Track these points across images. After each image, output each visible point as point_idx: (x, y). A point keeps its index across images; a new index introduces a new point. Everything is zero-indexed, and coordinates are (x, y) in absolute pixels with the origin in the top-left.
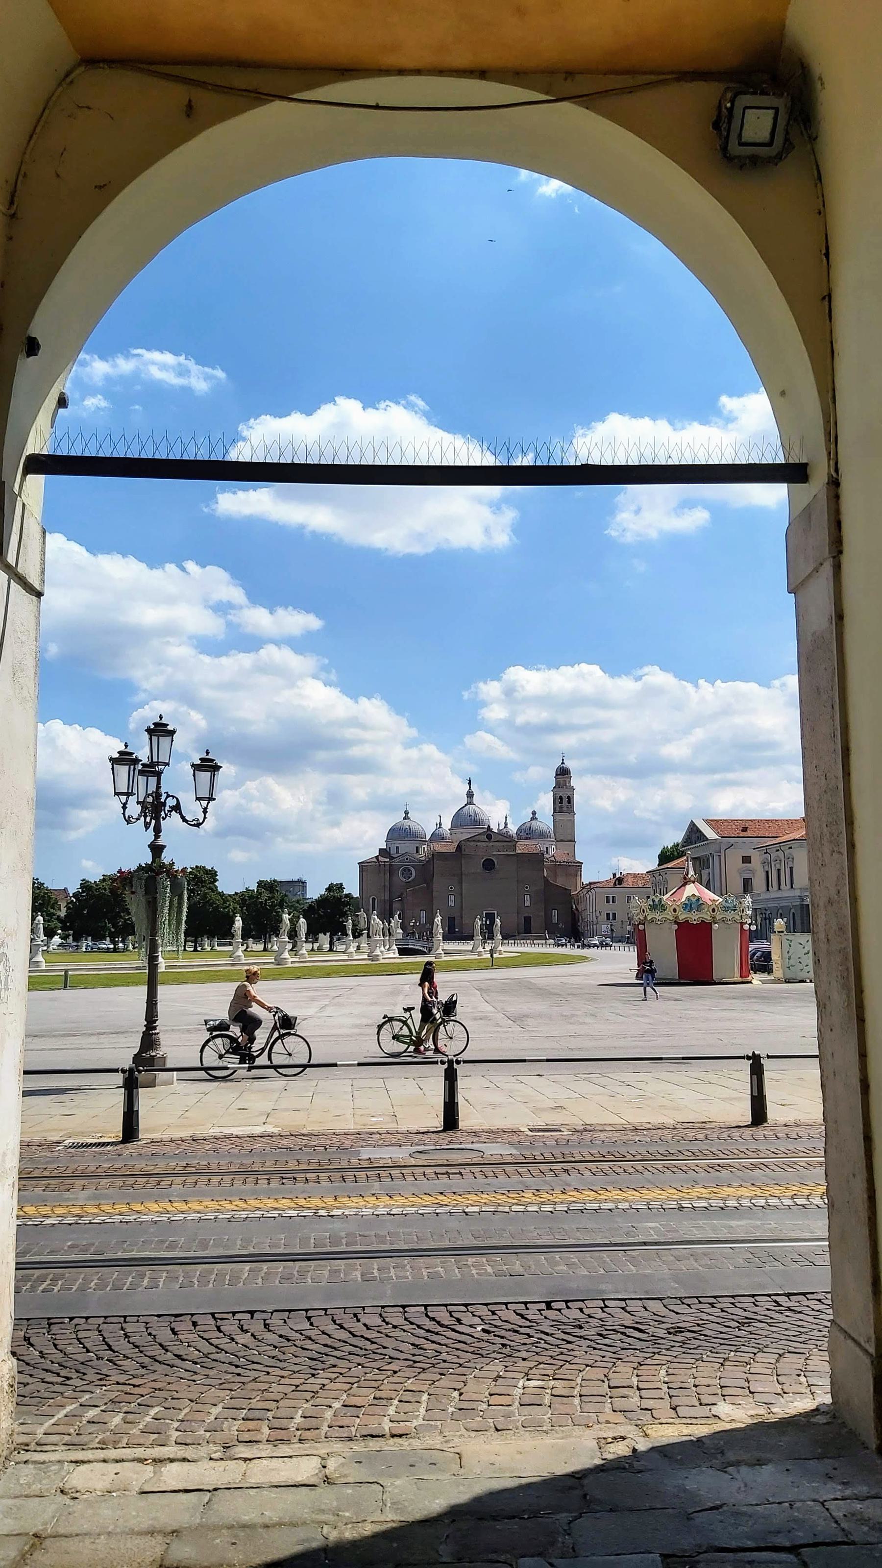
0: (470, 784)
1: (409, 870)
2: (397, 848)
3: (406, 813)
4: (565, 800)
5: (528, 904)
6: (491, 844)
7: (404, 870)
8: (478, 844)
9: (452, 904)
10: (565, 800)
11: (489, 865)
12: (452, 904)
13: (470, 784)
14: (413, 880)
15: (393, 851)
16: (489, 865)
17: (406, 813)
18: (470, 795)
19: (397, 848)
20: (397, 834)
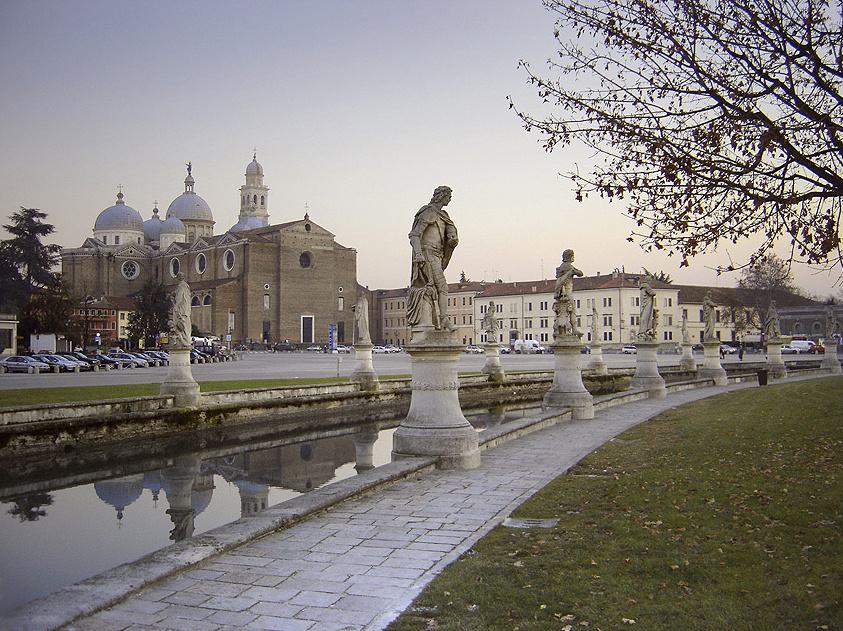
0: (189, 169)
1: (132, 266)
2: (117, 238)
3: (120, 196)
4: (259, 201)
5: (341, 308)
7: (126, 265)
9: (267, 306)
10: (259, 201)
11: (306, 259)
12: (267, 306)
13: (189, 169)
16: (306, 259)
17: (120, 196)
18: (189, 182)
19: (117, 238)
20: (106, 220)
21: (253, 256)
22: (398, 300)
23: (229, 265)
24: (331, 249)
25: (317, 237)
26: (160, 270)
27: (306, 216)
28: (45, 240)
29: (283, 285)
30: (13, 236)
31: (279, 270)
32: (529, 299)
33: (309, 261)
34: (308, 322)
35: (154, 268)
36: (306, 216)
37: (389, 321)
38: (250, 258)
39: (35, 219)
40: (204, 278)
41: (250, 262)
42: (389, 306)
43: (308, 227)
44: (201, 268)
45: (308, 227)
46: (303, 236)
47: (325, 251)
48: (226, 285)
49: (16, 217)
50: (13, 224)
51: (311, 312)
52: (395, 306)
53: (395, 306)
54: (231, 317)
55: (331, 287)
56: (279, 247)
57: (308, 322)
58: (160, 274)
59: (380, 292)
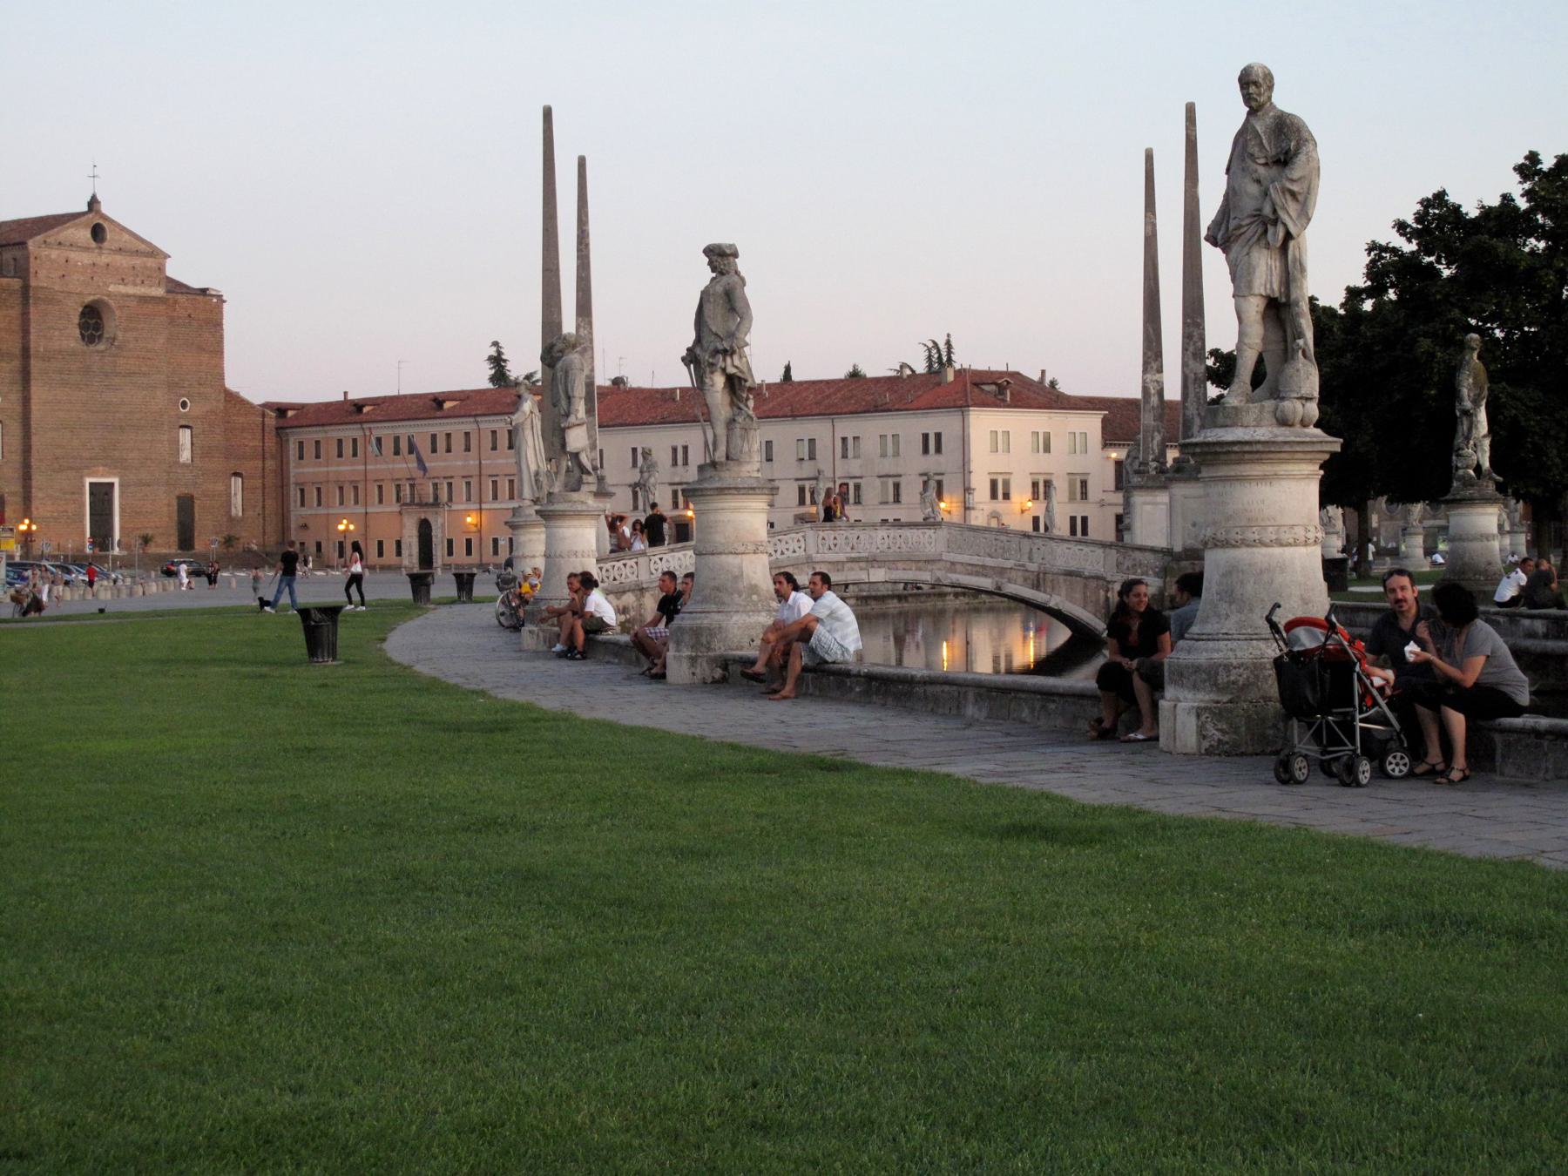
5: (185, 456)
6: (104, 259)
8: (74, 255)
11: (92, 318)
22: (335, 433)
24: (159, 292)
25: (118, 257)
27: (93, 203)
29: (38, 392)
31: (26, 353)
33: (98, 327)
34: (101, 495)
36: (93, 203)
37: (312, 495)
42: (310, 450)
43: (98, 232)
45: (98, 232)
46: (84, 258)
47: (143, 299)
56: (26, 288)
57: (101, 495)
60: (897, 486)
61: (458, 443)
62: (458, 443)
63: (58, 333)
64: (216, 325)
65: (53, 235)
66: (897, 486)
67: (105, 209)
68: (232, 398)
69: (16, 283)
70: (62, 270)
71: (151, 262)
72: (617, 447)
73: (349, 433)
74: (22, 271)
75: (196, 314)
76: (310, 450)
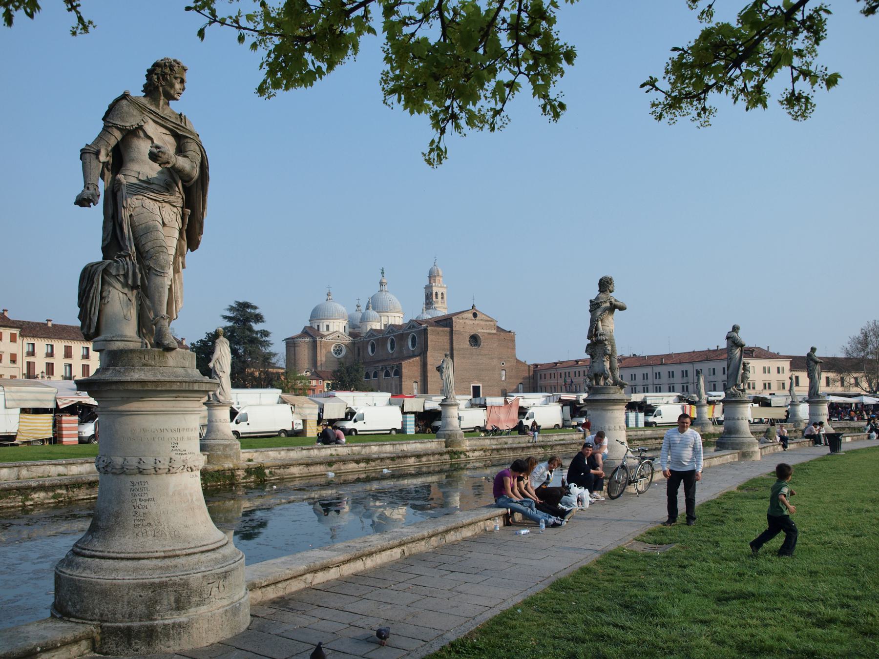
0: (383, 273)
2: (328, 326)
5: (503, 378)
6: (476, 322)
8: (467, 321)
10: (440, 296)
13: (383, 273)
14: (345, 357)
15: (323, 330)
16: (475, 340)
19: (328, 326)
21: (430, 338)
23: (413, 345)
24: (495, 331)
26: (361, 350)
28: (257, 327)
30: (230, 324)
32: (657, 369)
35: (356, 348)
38: (429, 340)
39: (249, 310)
40: (394, 356)
41: (429, 343)
42: (543, 376)
43: (475, 315)
44: (392, 348)
45: (475, 315)
46: (471, 322)
47: (489, 334)
48: (411, 360)
49: (232, 309)
50: (228, 314)
51: (480, 381)
52: (548, 376)
53: (548, 376)
54: (415, 385)
55: (495, 362)
58: (361, 353)
59: (536, 366)
60: (714, 385)
61: (582, 374)
62: (582, 374)
63: (462, 343)
64: (513, 341)
65: (460, 316)
66: (714, 385)
67: (477, 308)
68: (518, 361)
69: (448, 329)
70: (464, 326)
71: (491, 323)
72: (627, 373)
73: (553, 372)
74: (451, 327)
75: (505, 337)
76: (543, 376)
